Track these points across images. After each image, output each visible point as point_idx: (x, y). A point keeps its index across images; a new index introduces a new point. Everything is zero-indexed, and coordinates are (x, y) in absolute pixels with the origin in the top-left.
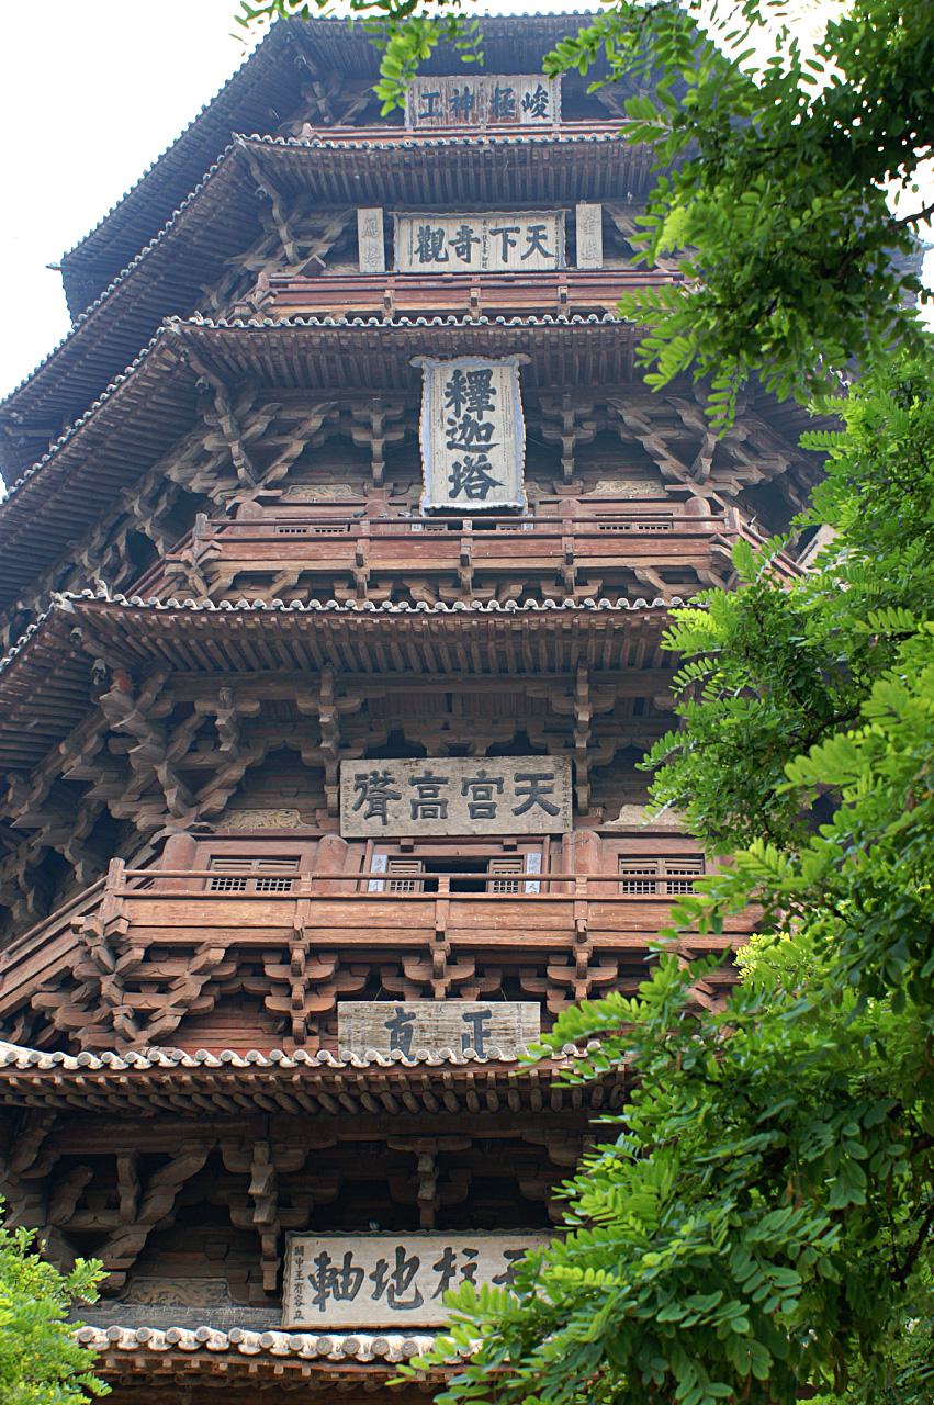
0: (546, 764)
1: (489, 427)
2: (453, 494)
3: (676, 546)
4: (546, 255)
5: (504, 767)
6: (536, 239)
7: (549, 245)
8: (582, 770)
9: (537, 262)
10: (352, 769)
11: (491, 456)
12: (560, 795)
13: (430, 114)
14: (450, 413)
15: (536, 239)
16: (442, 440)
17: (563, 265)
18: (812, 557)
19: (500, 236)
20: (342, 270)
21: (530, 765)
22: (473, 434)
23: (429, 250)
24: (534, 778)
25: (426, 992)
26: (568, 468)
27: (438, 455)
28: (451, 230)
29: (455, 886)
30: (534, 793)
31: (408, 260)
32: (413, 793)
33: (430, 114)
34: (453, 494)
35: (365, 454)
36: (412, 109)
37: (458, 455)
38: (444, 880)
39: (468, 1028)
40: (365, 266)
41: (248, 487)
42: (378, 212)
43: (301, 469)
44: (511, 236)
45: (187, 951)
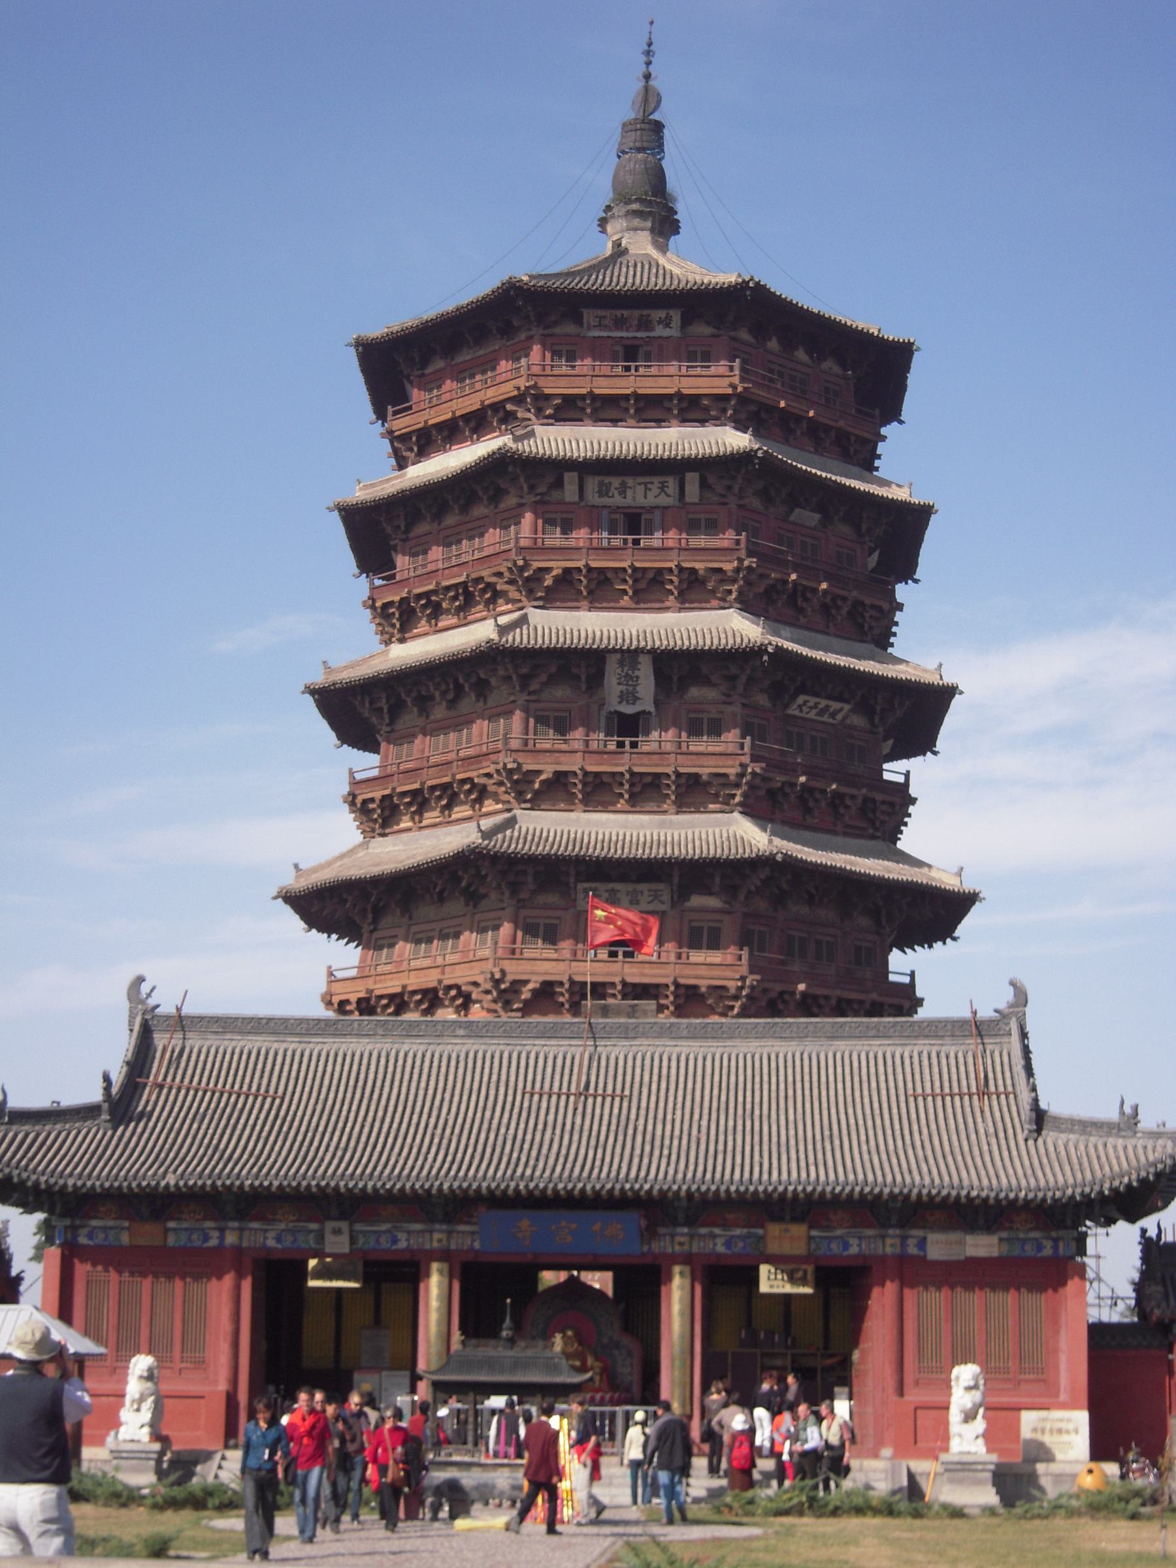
0: (661, 886)
1: (637, 677)
2: (620, 703)
3: (721, 761)
4: (668, 496)
5: (644, 887)
6: (663, 487)
7: (670, 491)
8: (675, 888)
9: (664, 500)
10: (581, 886)
11: (638, 688)
12: (666, 897)
13: (600, 325)
14: (619, 671)
15: (663, 487)
16: (614, 681)
17: (677, 504)
18: (795, 706)
19: (643, 486)
20: (555, 495)
21: (654, 886)
22: (630, 680)
23: (604, 491)
24: (656, 891)
25: (614, 996)
26: (675, 689)
27: (613, 685)
28: (616, 482)
29: (626, 955)
30: (656, 896)
31: (592, 497)
32: (606, 895)
33: (600, 325)
34: (620, 703)
35: (578, 677)
36: (589, 323)
37: (623, 688)
38: (621, 950)
39: (630, 1010)
40: (568, 499)
41: (522, 691)
42: (575, 474)
43: (545, 685)
44: (649, 486)
45: (526, 982)
